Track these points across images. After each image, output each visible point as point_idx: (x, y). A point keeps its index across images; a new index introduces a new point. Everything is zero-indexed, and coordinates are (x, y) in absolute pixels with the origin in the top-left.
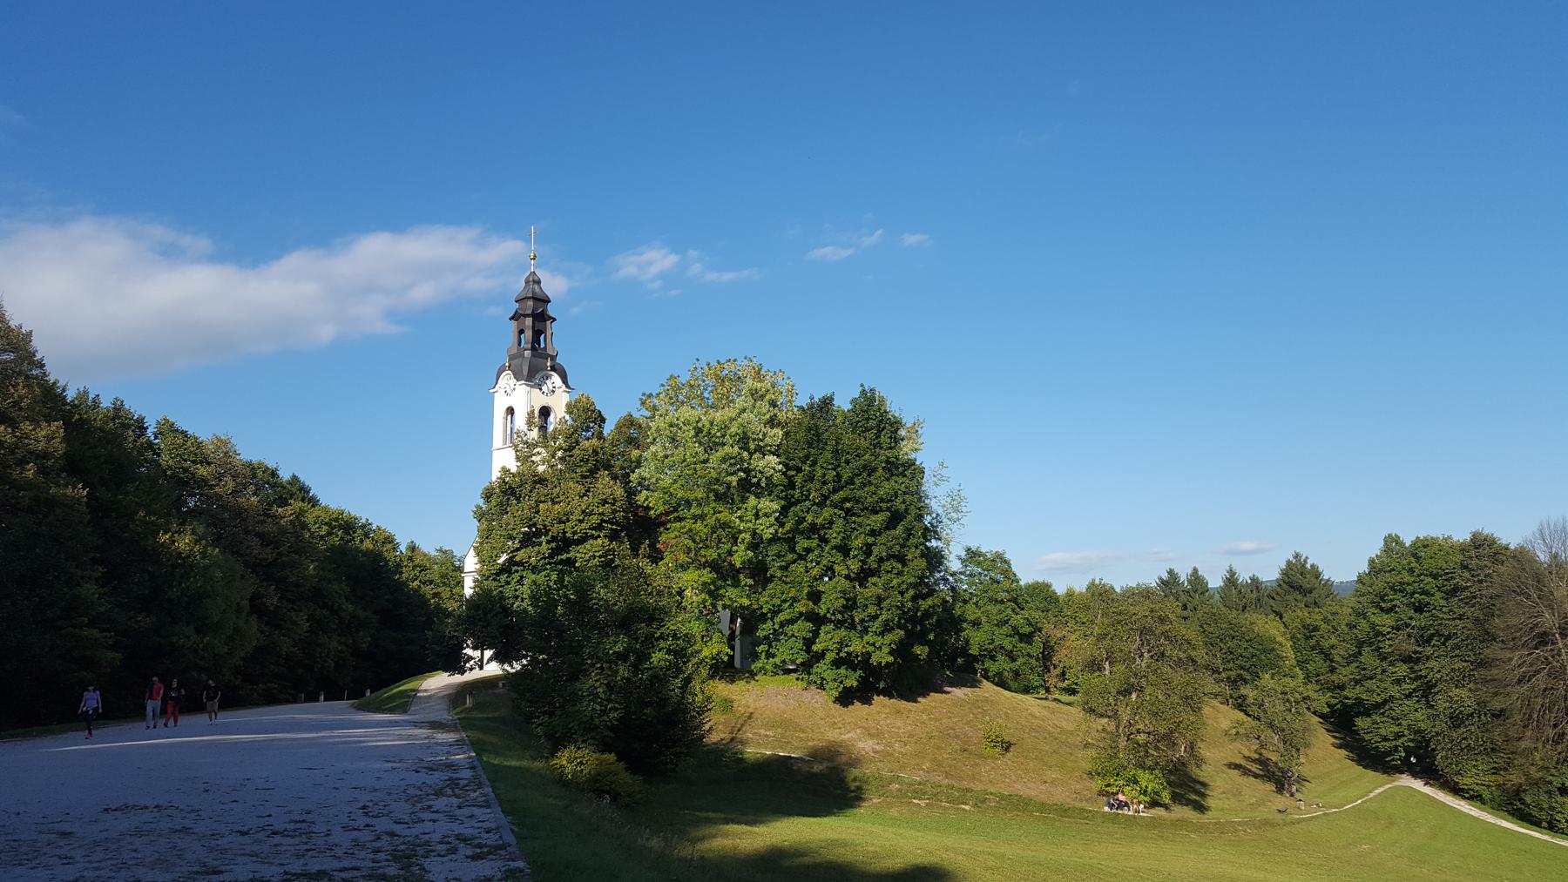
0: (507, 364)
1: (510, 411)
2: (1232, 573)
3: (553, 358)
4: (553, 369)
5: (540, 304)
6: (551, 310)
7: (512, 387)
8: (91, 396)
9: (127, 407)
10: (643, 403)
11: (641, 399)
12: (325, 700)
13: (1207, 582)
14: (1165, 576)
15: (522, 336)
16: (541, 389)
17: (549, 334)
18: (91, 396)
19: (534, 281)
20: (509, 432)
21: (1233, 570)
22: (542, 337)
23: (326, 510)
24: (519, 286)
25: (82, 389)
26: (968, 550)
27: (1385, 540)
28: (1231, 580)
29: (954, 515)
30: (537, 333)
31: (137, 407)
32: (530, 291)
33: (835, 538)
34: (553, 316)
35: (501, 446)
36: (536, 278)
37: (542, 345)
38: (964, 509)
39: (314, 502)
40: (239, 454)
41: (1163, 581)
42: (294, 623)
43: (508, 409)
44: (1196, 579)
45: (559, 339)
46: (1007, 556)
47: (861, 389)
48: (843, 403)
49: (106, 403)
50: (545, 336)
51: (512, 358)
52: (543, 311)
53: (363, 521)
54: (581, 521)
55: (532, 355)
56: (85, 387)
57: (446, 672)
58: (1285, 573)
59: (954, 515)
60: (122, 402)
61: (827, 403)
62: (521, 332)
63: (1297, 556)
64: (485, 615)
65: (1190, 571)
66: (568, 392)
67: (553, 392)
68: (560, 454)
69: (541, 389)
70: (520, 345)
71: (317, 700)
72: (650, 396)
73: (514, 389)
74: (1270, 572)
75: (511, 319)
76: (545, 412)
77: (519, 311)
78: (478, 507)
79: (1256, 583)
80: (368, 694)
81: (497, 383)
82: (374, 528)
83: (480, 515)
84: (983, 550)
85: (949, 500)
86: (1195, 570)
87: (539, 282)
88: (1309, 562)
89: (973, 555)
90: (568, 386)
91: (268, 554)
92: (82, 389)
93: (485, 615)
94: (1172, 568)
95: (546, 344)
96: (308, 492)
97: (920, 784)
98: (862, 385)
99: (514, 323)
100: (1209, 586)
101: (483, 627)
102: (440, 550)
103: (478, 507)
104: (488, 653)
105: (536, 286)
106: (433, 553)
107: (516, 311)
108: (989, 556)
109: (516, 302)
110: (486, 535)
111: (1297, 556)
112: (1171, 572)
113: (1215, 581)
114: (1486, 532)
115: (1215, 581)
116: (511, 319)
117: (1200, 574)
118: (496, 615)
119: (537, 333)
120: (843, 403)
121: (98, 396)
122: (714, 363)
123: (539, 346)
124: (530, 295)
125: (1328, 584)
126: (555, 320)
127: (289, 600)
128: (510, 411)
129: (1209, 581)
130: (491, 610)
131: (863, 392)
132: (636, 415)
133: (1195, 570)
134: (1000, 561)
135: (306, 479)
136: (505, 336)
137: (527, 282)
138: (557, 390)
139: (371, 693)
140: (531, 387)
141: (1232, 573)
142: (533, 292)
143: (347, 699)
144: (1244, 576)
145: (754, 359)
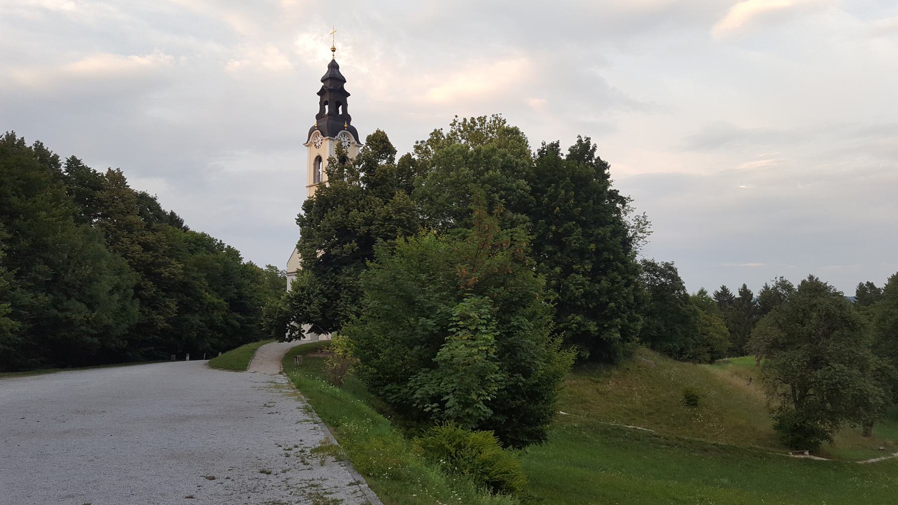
1: (319, 159)
3: (349, 123)
6: (347, 87)
7: (320, 142)
8: (18, 137)
9: (45, 148)
10: (417, 148)
11: (415, 146)
12: (190, 359)
13: (752, 294)
14: (720, 290)
18: (18, 137)
20: (317, 174)
21: (768, 285)
22: (340, 108)
23: (193, 233)
24: (324, 70)
25: (10, 133)
26: (644, 261)
29: (640, 235)
31: (52, 147)
32: (332, 73)
33: (575, 243)
35: (312, 183)
37: (341, 113)
38: (648, 230)
39: (186, 229)
40: (128, 186)
42: (167, 306)
45: (353, 106)
46: (675, 266)
47: (577, 139)
48: (564, 152)
49: (29, 143)
53: (219, 241)
54: (382, 225)
56: (12, 132)
57: (277, 339)
59: (640, 235)
60: (42, 144)
61: (554, 147)
62: (326, 103)
63: (811, 278)
64: (309, 295)
65: (741, 287)
68: (362, 174)
71: (185, 360)
72: (422, 142)
73: (321, 143)
75: (318, 94)
78: (300, 216)
80: (220, 354)
82: (226, 247)
83: (301, 221)
84: (656, 262)
85: (637, 222)
86: (745, 286)
87: (337, 67)
89: (650, 267)
91: (148, 257)
92: (10, 133)
93: (309, 295)
94: (724, 285)
96: (182, 224)
97: (656, 436)
98: (579, 136)
99: (319, 97)
101: (307, 304)
102: (269, 266)
103: (300, 216)
104: (306, 327)
105: (336, 70)
106: (265, 268)
107: (322, 88)
108: (659, 265)
109: (322, 81)
110: (306, 236)
111: (811, 278)
112: (723, 288)
113: (756, 294)
116: (318, 94)
118: (316, 296)
120: (564, 152)
121: (23, 138)
122: (469, 121)
124: (331, 76)
126: (349, 95)
127: (163, 290)
129: (754, 293)
130: (312, 292)
131: (580, 141)
132: (413, 157)
133: (745, 286)
134: (669, 271)
135: (180, 214)
136: (313, 105)
137: (329, 66)
138: (351, 145)
139: (222, 353)
140: (333, 140)
143: (205, 359)
145: (499, 116)
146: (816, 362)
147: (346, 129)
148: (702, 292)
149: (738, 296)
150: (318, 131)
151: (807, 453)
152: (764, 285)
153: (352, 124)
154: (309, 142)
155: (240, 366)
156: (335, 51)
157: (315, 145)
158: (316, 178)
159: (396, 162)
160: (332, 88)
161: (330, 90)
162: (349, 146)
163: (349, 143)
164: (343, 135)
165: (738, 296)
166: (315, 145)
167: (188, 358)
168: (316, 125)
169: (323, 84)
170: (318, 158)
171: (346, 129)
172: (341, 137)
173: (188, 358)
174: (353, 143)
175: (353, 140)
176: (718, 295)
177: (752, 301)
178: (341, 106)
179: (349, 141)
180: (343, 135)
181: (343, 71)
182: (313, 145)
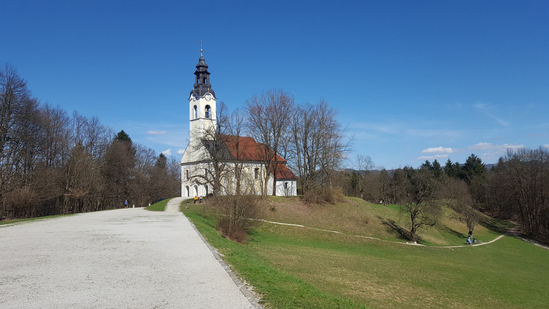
2: (449, 161)
5: (204, 68)
6: (209, 70)
12: (135, 207)
14: (425, 163)
16: (206, 99)
17: (208, 78)
19: (202, 60)
20: (195, 114)
21: (450, 160)
24: (197, 63)
28: (449, 164)
30: (204, 79)
34: (210, 72)
36: (203, 59)
37: (206, 83)
41: (423, 165)
44: (436, 163)
45: (212, 80)
51: (195, 88)
52: (206, 71)
55: (203, 87)
58: (467, 161)
63: (473, 155)
65: (434, 161)
66: (215, 100)
67: (210, 100)
69: (206, 99)
70: (198, 82)
71: (132, 207)
74: (462, 161)
76: (208, 107)
77: (198, 71)
79: (457, 164)
81: (190, 97)
86: (436, 160)
88: (477, 157)
90: (215, 98)
95: (207, 83)
100: (441, 166)
105: (203, 62)
107: (196, 71)
109: (196, 67)
111: (473, 155)
112: (427, 162)
115: (443, 164)
116: (194, 74)
117: (437, 162)
125: (484, 166)
126: (209, 74)
128: (195, 107)
133: (436, 160)
137: (200, 60)
138: (211, 99)
139: (151, 205)
140: (203, 98)
141: (449, 161)
142: (202, 64)
144: (453, 162)
150: (195, 93)
151: (416, 242)
152: (448, 160)
153: (211, 88)
154: (190, 98)
155: (162, 209)
160: (201, 71)
161: (201, 72)
162: (210, 100)
163: (210, 98)
167: (134, 206)
170: (195, 107)
173: (134, 206)
174: (212, 98)
175: (212, 96)
177: (440, 169)
182: (193, 100)
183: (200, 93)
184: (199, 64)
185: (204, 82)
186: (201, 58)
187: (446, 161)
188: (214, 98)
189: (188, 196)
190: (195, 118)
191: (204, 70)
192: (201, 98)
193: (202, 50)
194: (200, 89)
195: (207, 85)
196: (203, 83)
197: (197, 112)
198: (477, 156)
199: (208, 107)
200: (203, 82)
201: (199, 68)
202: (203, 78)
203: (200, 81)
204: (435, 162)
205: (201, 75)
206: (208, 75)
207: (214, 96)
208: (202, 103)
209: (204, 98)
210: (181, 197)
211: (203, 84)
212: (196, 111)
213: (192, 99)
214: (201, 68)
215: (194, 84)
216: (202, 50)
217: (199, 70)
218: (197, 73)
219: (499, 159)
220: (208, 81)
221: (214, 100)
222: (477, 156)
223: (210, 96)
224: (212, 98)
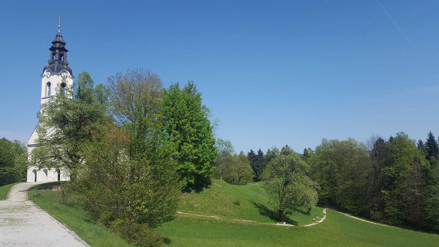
0: (48, 66)
3: (67, 65)
4: (66, 69)
5: (61, 45)
6: (66, 47)
13: (263, 153)
14: (250, 152)
15: (54, 56)
16: (62, 76)
17: (65, 56)
19: (60, 36)
20: (48, 92)
21: (270, 150)
22: (62, 58)
24: (53, 39)
27: (323, 140)
30: (61, 55)
35: (44, 97)
36: (61, 35)
37: (62, 60)
41: (249, 153)
43: (48, 82)
44: (260, 152)
45: (69, 57)
50: (64, 57)
51: (50, 64)
62: (54, 54)
63: (287, 146)
65: (259, 150)
67: (67, 77)
70: (53, 59)
75: (50, 49)
81: (43, 73)
84: (223, 139)
86: (260, 149)
87: (62, 37)
90: (72, 76)
95: (64, 60)
100: (264, 154)
102: (15, 141)
105: (60, 38)
107: (52, 46)
109: (52, 43)
112: (251, 151)
113: (265, 153)
114: (352, 138)
116: (50, 49)
117: (261, 151)
119: (61, 55)
123: (61, 60)
124: (59, 41)
126: (67, 51)
128: (49, 84)
133: (260, 149)
137: (57, 36)
138: (68, 77)
140: (58, 75)
142: (59, 40)
146: (286, 183)
147: (65, 68)
148: (242, 152)
149: (257, 154)
151: (285, 223)
153: (69, 66)
154: (43, 75)
156: (60, 28)
157: (47, 76)
158: (47, 93)
159: (94, 87)
160: (58, 47)
161: (57, 48)
163: (67, 76)
164: (63, 72)
165: (257, 154)
166: (47, 76)
168: (48, 66)
169: (52, 44)
170: (48, 84)
171: (65, 68)
172: (62, 72)
174: (69, 76)
175: (69, 74)
176: (249, 154)
178: (63, 56)
179: (67, 75)
180: (63, 72)
181: (64, 39)
182: (46, 76)
183: (56, 69)
184: (55, 40)
185: (61, 59)
186: (58, 34)
187: (267, 151)
188: (71, 76)
189: (36, 181)
190: (47, 96)
191: (62, 47)
192: (56, 74)
193: (59, 26)
194: (56, 65)
195: (64, 62)
196: (59, 59)
197: (51, 90)
198: (290, 147)
199: (63, 85)
200: (59, 58)
201: (55, 44)
202: (59, 54)
203: (56, 57)
204: (259, 151)
205: (57, 51)
206: (65, 52)
207: (71, 74)
208: (56, 80)
209: (60, 76)
210: (25, 181)
211: (60, 61)
212: (49, 89)
213: (45, 75)
214: (57, 44)
215: (48, 60)
216: (59, 26)
217: (56, 46)
218: (52, 49)
219: (304, 149)
220: (65, 58)
221: (71, 78)
222: (290, 147)
223: (66, 74)
224: (69, 76)
